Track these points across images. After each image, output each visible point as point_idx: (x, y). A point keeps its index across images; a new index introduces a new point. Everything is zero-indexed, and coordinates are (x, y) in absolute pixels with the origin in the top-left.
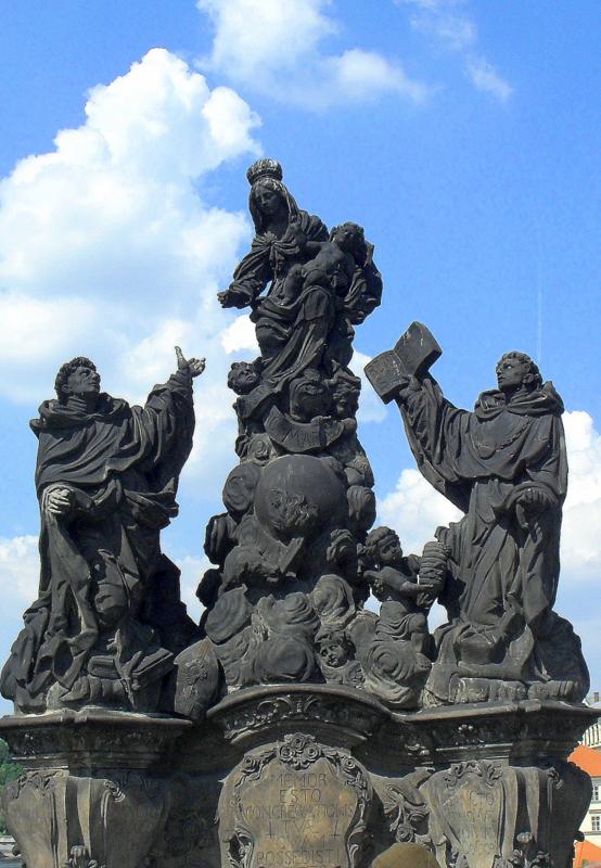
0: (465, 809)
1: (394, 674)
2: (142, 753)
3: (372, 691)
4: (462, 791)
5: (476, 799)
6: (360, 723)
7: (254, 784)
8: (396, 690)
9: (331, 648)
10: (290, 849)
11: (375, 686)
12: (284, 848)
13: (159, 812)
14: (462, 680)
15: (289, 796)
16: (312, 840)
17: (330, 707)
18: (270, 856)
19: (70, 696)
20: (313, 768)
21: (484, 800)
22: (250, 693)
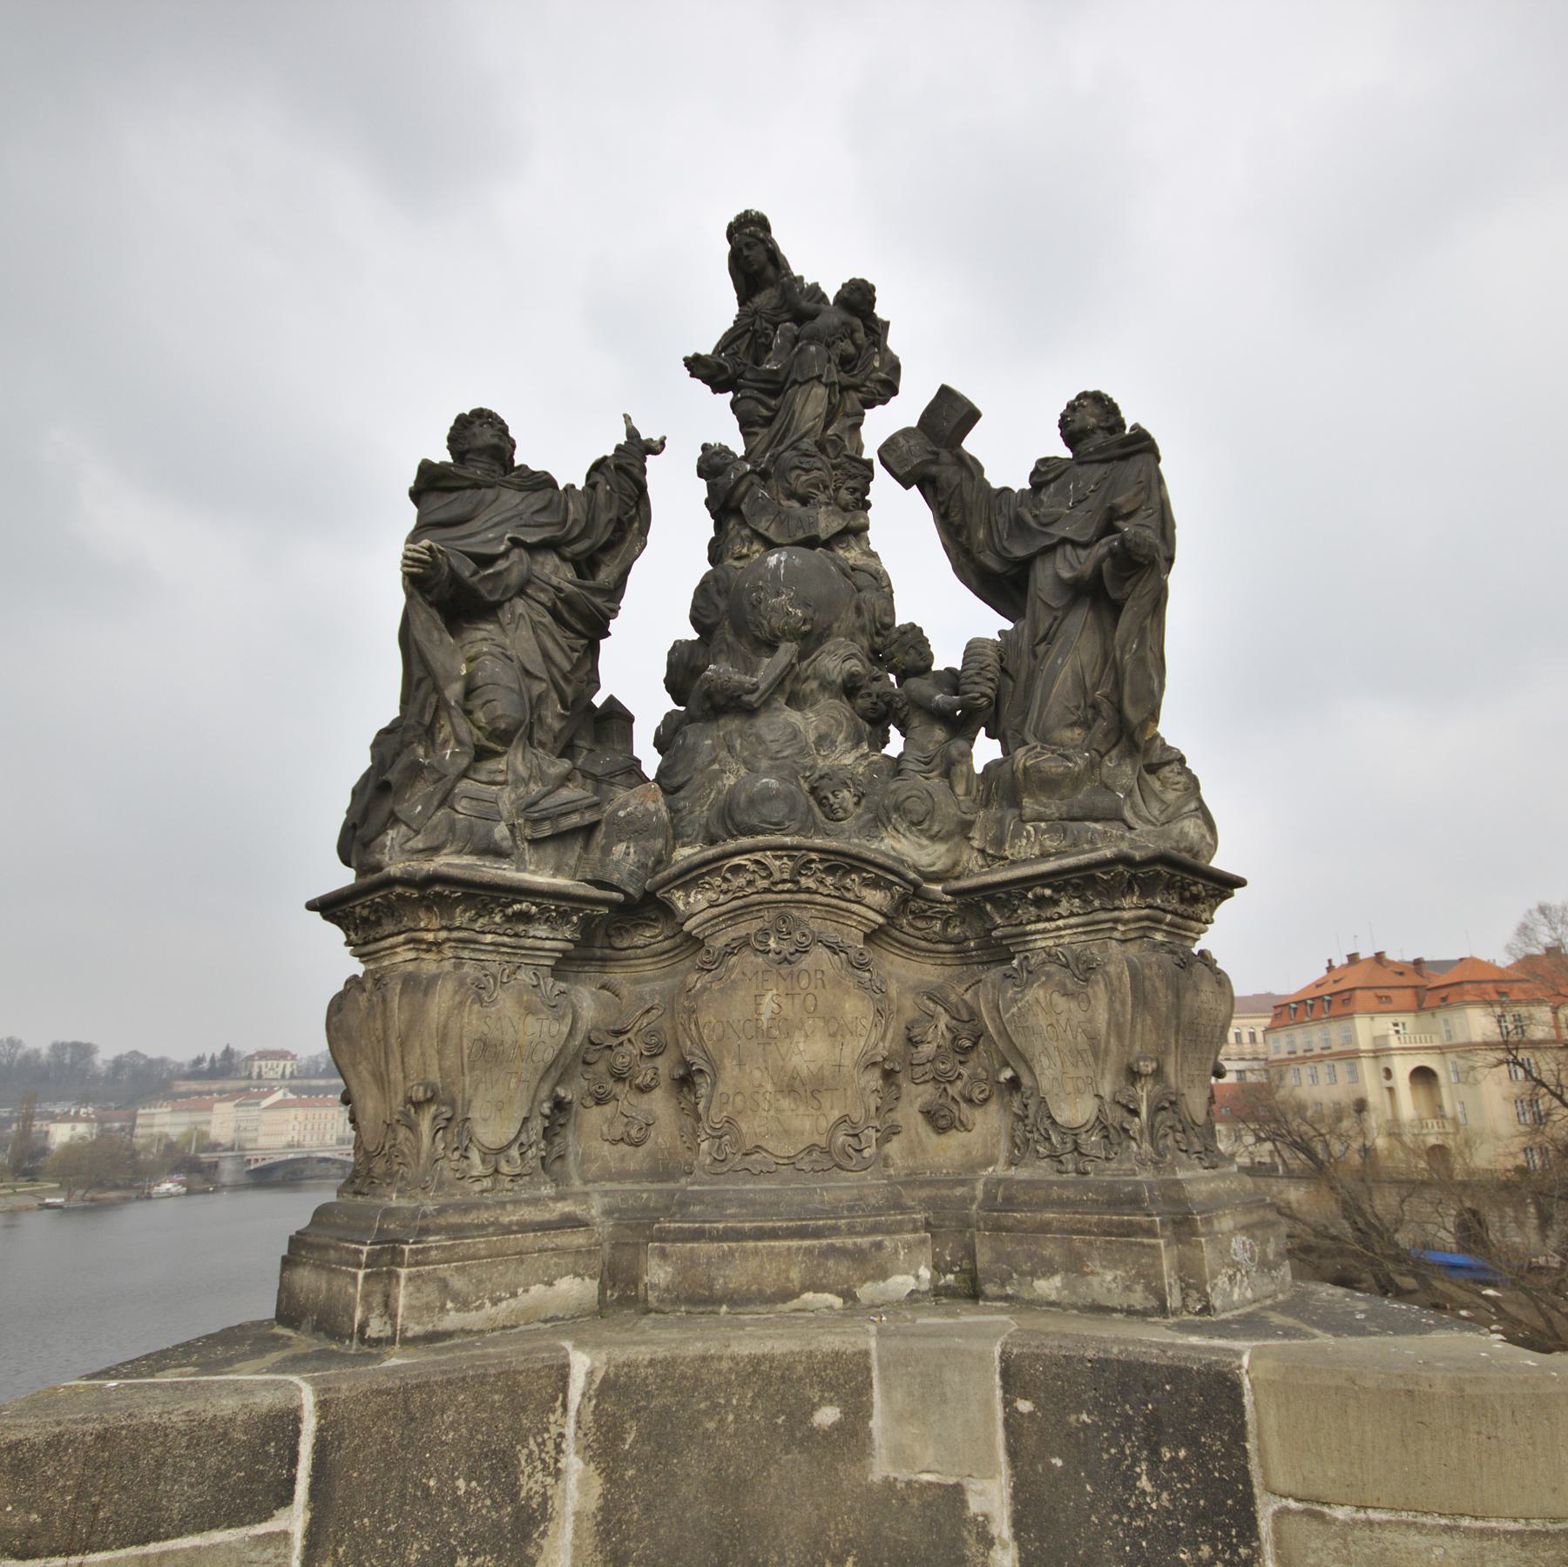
0: (1042, 1020)
1: (925, 826)
2: (541, 938)
3: (893, 853)
4: (1037, 993)
5: (1061, 1003)
6: (876, 897)
7: (715, 986)
8: (930, 850)
9: (833, 793)
10: (769, 1087)
11: (897, 846)
12: (761, 1085)
13: (566, 1030)
14: (1029, 827)
15: (768, 1004)
16: (804, 1073)
17: (831, 870)
18: (739, 1098)
19: (418, 842)
20: (806, 962)
21: (1073, 1005)
22: (712, 852)
